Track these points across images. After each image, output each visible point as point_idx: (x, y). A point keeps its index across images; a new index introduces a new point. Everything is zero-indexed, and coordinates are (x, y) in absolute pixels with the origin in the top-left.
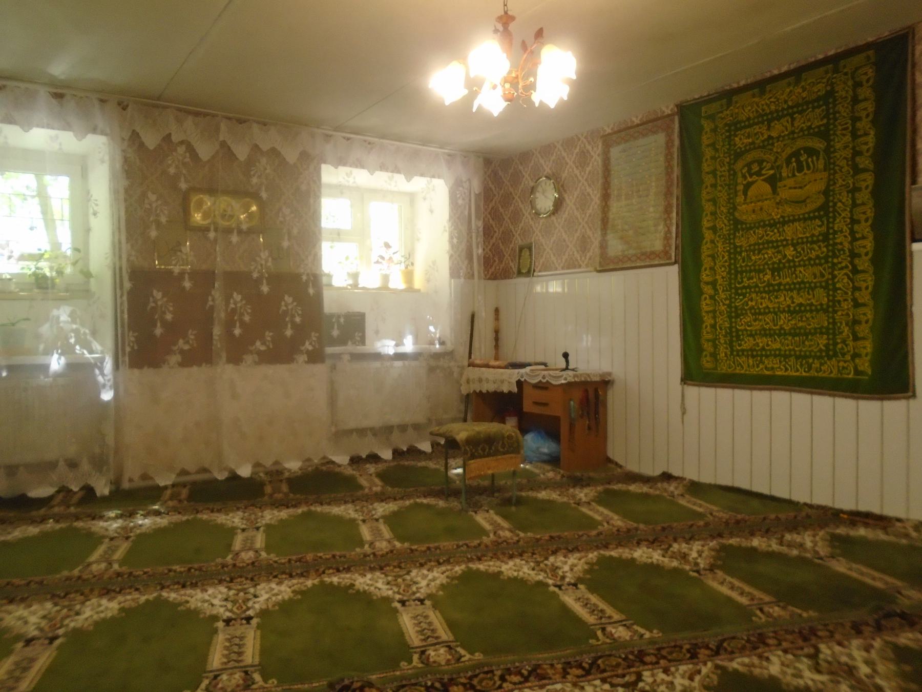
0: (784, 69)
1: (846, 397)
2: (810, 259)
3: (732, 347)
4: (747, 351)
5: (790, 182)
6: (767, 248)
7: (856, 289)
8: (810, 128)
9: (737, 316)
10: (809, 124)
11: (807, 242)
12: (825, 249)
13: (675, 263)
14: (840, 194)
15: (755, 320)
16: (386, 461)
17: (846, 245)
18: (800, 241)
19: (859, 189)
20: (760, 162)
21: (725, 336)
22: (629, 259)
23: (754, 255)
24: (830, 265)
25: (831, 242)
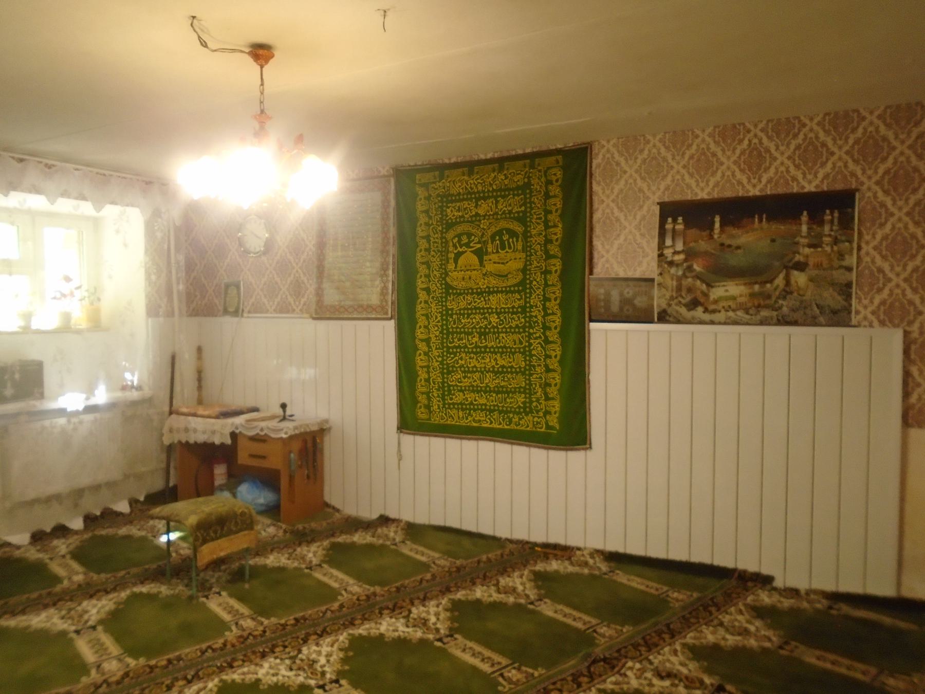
0: (489, 156)
1: (539, 447)
2: (511, 327)
3: (444, 399)
4: (458, 404)
5: (494, 257)
6: (476, 314)
8: (510, 212)
9: (449, 373)
11: (509, 312)
13: (390, 319)
15: (464, 378)
16: (76, 532)
17: (540, 318)
20: (469, 235)
21: (438, 390)
22: (346, 310)
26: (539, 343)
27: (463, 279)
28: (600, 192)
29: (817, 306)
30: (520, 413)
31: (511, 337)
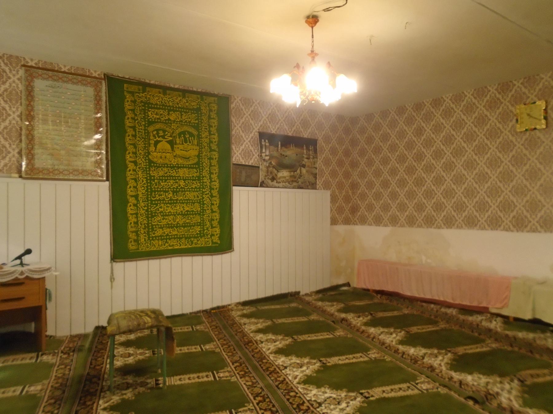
2: (192, 188)
3: (149, 234)
4: (158, 237)
5: (181, 147)
6: (170, 179)
7: (213, 204)
8: (190, 122)
9: (152, 217)
11: (191, 179)
15: (163, 219)
17: (208, 183)
19: (213, 159)
20: (164, 131)
21: (144, 229)
23: (162, 182)
27: (161, 157)
28: (234, 121)
29: (309, 182)
30: (198, 237)
31: (192, 194)
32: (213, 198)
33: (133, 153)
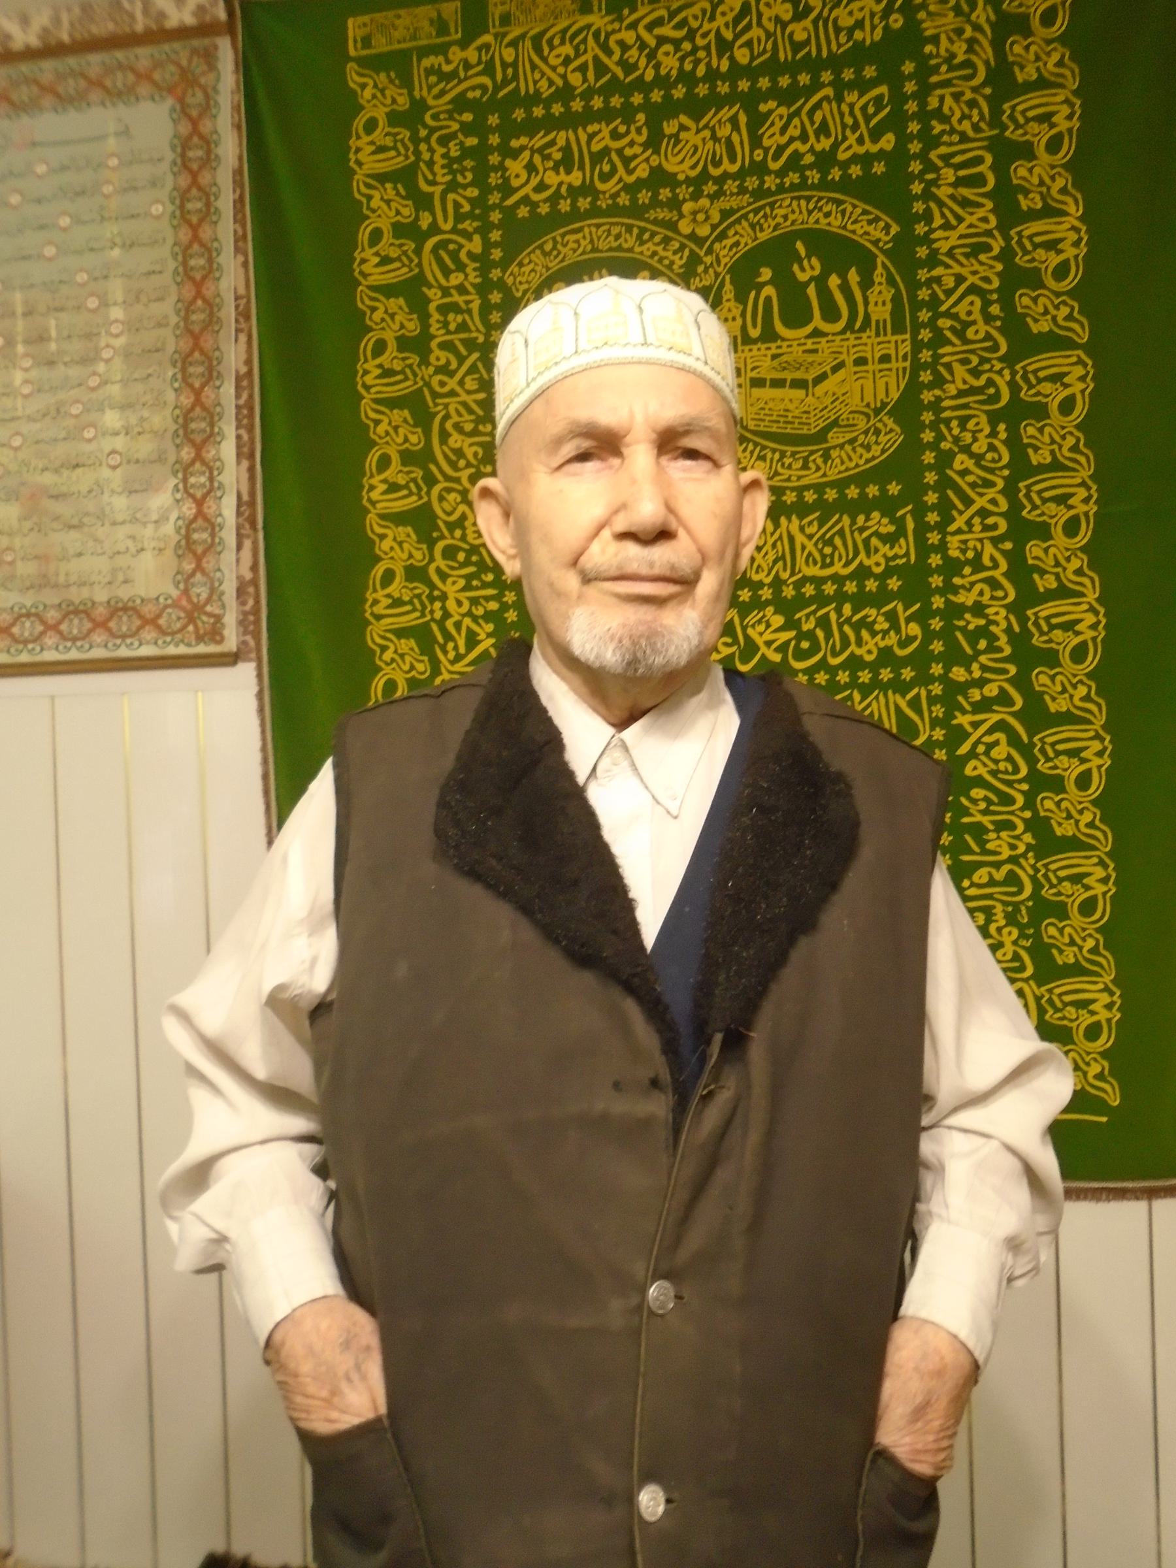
2: (854, 663)
7: (1043, 783)
8: (825, 160)
10: (825, 144)
11: (840, 598)
12: (914, 629)
13: (231, 659)
14: (963, 421)
17: (998, 613)
18: (809, 590)
19: (1039, 412)
24: (937, 689)
25: (938, 602)
26: (1000, 726)
32: (1051, 735)
33: (408, 458)
